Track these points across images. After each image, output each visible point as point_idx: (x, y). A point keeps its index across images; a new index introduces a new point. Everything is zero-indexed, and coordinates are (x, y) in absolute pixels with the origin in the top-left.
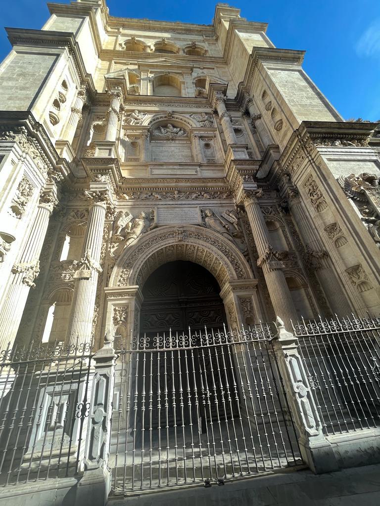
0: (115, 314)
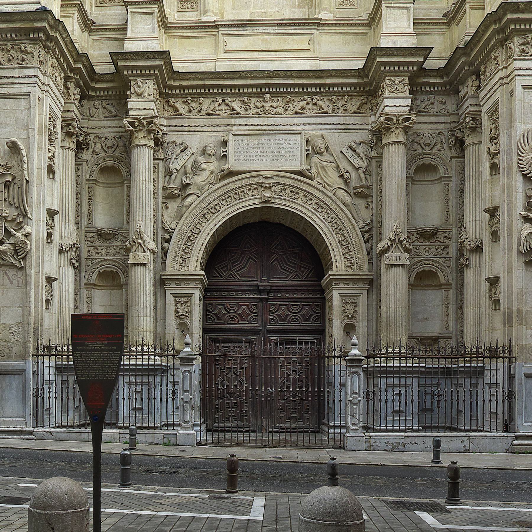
0: (176, 306)
